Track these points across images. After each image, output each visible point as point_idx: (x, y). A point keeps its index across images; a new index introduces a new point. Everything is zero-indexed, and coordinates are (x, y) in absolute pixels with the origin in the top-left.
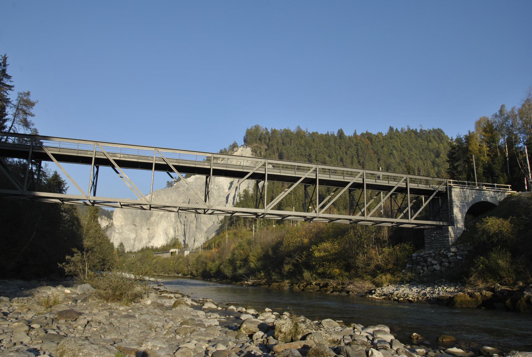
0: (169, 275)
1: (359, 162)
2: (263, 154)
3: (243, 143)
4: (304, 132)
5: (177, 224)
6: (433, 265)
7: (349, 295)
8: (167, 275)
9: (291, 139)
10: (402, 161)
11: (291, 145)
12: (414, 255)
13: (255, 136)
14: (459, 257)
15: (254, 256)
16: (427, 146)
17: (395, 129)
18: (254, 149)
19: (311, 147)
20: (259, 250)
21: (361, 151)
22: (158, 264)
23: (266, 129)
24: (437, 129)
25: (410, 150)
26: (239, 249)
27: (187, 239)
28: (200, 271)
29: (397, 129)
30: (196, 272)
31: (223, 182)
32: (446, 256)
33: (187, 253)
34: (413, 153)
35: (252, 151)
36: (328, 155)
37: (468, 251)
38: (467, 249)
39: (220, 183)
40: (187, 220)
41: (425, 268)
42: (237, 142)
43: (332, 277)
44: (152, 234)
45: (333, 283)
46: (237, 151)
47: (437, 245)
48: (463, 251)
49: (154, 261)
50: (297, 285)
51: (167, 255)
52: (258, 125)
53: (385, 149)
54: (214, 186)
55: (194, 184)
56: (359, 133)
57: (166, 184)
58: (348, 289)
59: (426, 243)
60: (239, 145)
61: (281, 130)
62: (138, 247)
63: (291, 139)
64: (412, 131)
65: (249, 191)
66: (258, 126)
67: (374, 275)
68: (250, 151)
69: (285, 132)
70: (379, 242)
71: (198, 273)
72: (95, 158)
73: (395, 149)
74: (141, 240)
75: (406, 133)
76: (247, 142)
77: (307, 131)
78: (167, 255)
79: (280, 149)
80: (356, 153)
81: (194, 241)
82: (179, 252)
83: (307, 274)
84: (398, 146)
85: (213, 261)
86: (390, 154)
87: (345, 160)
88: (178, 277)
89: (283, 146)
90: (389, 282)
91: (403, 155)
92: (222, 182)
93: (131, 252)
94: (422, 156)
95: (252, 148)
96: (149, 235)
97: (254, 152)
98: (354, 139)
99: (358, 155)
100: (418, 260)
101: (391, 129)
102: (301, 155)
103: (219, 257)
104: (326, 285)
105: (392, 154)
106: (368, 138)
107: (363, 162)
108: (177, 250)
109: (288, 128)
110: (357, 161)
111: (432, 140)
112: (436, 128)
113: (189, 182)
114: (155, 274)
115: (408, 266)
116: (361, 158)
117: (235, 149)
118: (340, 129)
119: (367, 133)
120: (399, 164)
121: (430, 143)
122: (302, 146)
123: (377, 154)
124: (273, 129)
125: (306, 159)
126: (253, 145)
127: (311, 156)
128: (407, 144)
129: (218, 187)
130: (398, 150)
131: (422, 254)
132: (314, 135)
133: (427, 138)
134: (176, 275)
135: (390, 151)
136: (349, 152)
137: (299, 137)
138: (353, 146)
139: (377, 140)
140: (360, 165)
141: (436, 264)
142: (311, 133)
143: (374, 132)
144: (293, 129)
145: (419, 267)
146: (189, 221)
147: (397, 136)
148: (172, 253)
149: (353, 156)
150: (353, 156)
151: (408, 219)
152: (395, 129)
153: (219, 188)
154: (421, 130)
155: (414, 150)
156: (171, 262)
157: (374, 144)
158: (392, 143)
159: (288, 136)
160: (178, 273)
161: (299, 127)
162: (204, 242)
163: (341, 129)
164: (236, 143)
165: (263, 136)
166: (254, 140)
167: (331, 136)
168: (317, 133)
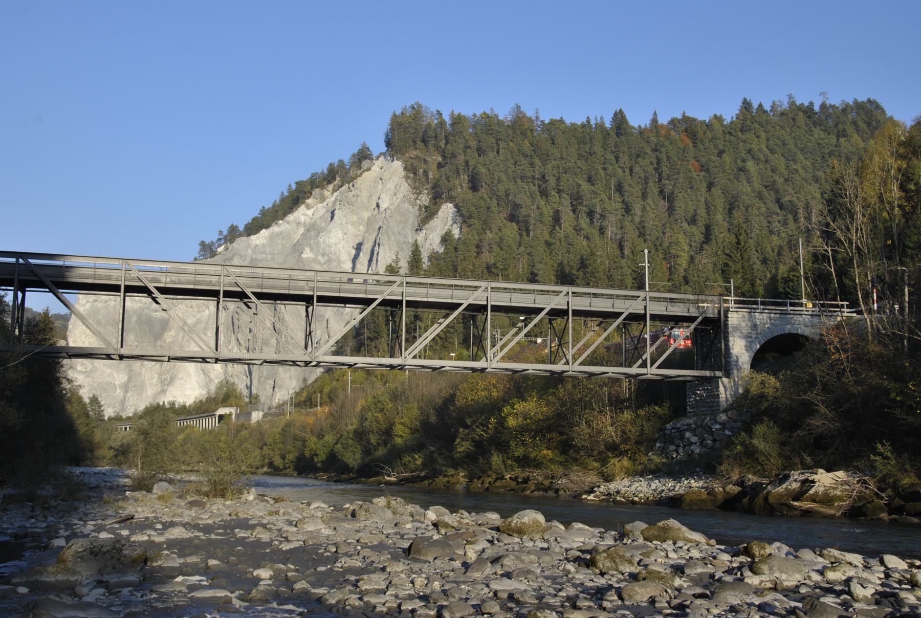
1: (661, 192)
2: (431, 176)
3: (384, 149)
4: (530, 119)
5: (230, 347)
6: (691, 443)
7: (558, 497)
9: (500, 139)
10: (766, 187)
11: (498, 153)
12: (668, 426)
13: (412, 131)
14: (727, 432)
16: (836, 146)
17: (755, 105)
18: (412, 165)
19: (545, 160)
20: (415, 412)
21: (669, 165)
22: (189, 445)
23: (439, 113)
24: (865, 100)
25: (790, 158)
26: (373, 411)
27: (255, 382)
28: (291, 457)
29: (760, 106)
30: (282, 461)
31: (338, 246)
32: (710, 432)
33: (256, 416)
34: (798, 166)
35: (405, 169)
37: (742, 421)
38: (743, 419)
40: (254, 336)
41: (681, 450)
43: (538, 465)
44: (168, 372)
46: (369, 169)
48: (735, 421)
49: (181, 437)
50: (480, 481)
51: (210, 423)
52: (420, 103)
53: (727, 158)
55: (267, 250)
56: (663, 120)
57: (198, 248)
58: (556, 487)
59: (689, 405)
60: (375, 153)
61: (475, 115)
62: (137, 404)
64: (800, 108)
66: (420, 106)
67: (604, 461)
68: (401, 169)
69: (483, 122)
70: (617, 404)
71: (286, 461)
73: (753, 158)
74: (141, 388)
75: (783, 114)
76: (393, 146)
78: (210, 423)
79: (472, 163)
80: (655, 169)
81: (274, 387)
82: (238, 416)
83: (496, 459)
84: (760, 150)
85: (320, 436)
86: (741, 169)
87: (626, 188)
89: (480, 156)
90: (626, 473)
91: (770, 174)
92: (336, 244)
93: (118, 419)
94: (820, 174)
95: (405, 162)
96: (161, 374)
97: (409, 170)
98: (651, 134)
99: (660, 175)
100: (673, 435)
101: (746, 105)
102: (521, 178)
103: (333, 427)
104: (526, 481)
105: (743, 171)
106: (686, 131)
107: (673, 193)
110: (656, 191)
111: (850, 129)
112: (862, 98)
115: (658, 445)
116: (667, 182)
117: (365, 164)
119: (685, 119)
120: (760, 196)
121: (842, 140)
122: (525, 156)
123: (708, 171)
124: (456, 113)
125: (534, 188)
127: (547, 181)
128: (784, 144)
129: (326, 258)
130: (759, 159)
131: (679, 425)
132: (555, 125)
133: (836, 125)
135: (740, 164)
136: (637, 169)
137: (518, 132)
138: (648, 151)
139: (709, 134)
140: (664, 199)
141: (695, 443)
142: (547, 122)
143: (702, 114)
144: (504, 113)
145: (673, 447)
146: (260, 340)
147: (760, 124)
148: (221, 417)
149: (646, 178)
150: (646, 178)
151: (646, 367)
152: (755, 105)
154: (823, 106)
155: (801, 157)
157: (700, 146)
158: (745, 142)
159: (491, 132)
161: (518, 107)
162: (297, 390)
163: (621, 110)
164: (368, 149)
165: (431, 133)
166: (411, 143)
167: (596, 128)
168: (561, 121)
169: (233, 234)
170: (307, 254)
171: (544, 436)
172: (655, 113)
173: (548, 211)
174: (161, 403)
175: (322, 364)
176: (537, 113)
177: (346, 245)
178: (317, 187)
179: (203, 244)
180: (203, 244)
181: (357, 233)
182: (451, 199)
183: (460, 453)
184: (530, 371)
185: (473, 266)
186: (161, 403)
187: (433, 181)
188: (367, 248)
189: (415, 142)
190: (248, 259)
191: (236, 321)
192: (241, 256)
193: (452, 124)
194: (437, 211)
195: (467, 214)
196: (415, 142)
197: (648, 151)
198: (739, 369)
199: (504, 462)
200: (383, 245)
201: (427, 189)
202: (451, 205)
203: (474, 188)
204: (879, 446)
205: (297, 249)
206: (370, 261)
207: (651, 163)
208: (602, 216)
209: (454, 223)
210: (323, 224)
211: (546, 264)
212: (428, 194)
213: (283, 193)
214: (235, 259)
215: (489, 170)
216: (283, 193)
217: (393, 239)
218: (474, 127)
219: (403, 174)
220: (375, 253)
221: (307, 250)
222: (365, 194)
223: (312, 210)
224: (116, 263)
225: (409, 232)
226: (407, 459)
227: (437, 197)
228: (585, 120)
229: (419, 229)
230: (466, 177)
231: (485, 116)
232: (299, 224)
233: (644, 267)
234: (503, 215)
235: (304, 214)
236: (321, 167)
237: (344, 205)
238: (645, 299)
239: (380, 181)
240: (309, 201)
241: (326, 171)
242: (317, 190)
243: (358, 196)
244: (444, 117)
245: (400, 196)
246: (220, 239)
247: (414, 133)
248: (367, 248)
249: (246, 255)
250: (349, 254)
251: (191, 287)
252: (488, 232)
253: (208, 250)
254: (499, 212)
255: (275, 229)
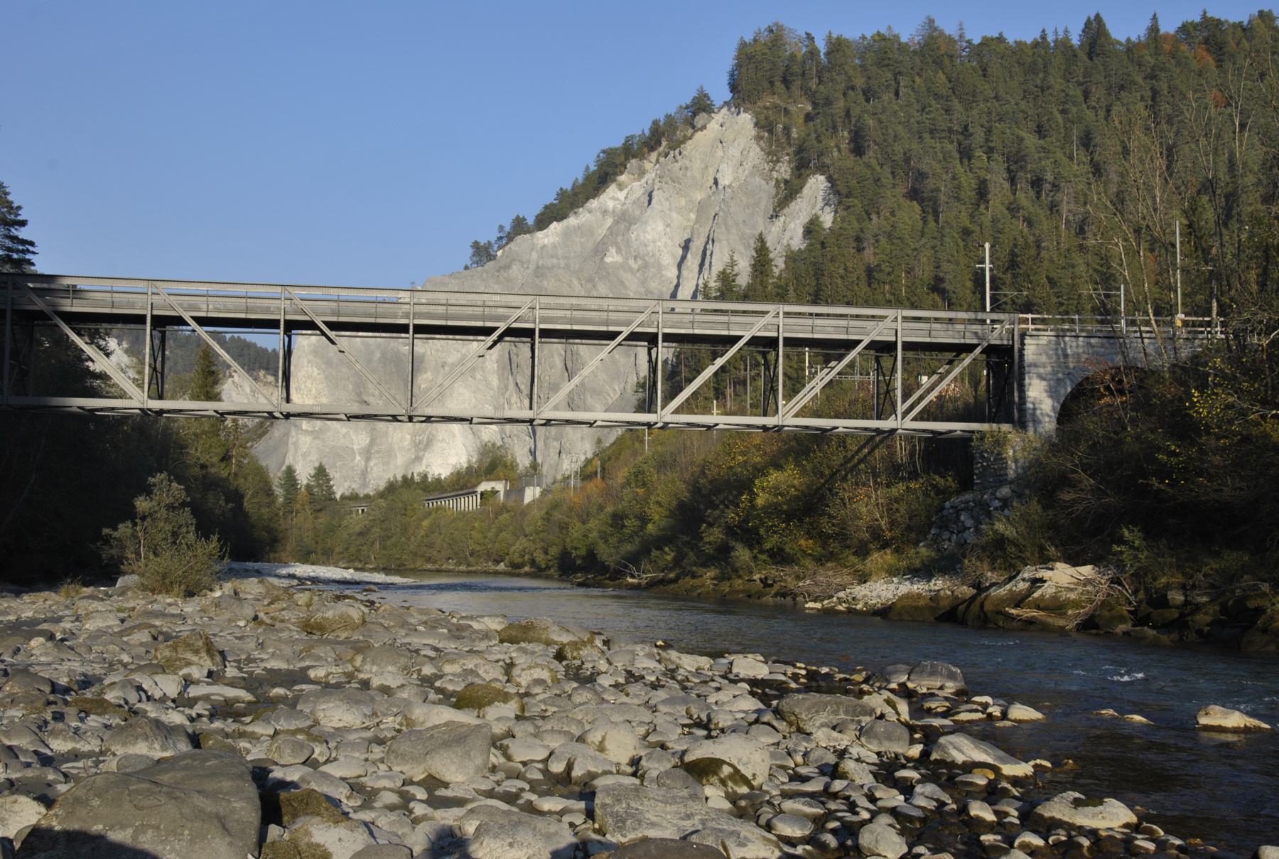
0: (470, 568)
2: (794, 135)
3: (728, 96)
4: (950, 40)
5: (507, 395)
8: (463, 568)
9: (900, 73)
11: (897, 94)
13: (767, 66)
15: (661, 506)
18: (766, 119)
19: (970, 99)
27: (540, 445)
28: (554, 551)
31: (659, 244)
33: (531, 494)
35: (756, 125)
36: (1032, 125)
39: (646, 246)
42: (707, 90)
45: (786, 575)
46: (704, 128)
49: (426, 523)
51: (469, 504)
52: (780, 23)
54: (627, 259)
55: (560, 252)
56: (1169, 26)
57: (470, 251)
60: (718, 102)
61: (864, 38)
62: (379, 476)
63: (900, 73)
65: (736, 275)
69: (877, 45)
70: (895, 471)
72: (153, 316)
74: (389, 454)
77: (961, 36)
78: (469, 504)
79: (855, 111)
81: (560, 452)
82: (507, 493)
83: (742, 554)
87: (1098, 140)
88: (497, 573)
89: (868, 100)
92: (654, 242)
93: (354, 497)
95: (756, 114)
97: (762, 127)
98: (1146, 52)
102: (931, 132)
108: (499, 486)
109: (890, 28)
113: (544, 246)
114: (429, 566)
115: (933, 531)
117: (700, 120)
118: (1092, 18)
122: (937, 97)
124: (835, 36)
125: (950, 147)
126: (759, 104)
127: (971, 135)
129: (640, 262)
134: (491, 566)
137: (930, 60)
138: (1139, 79)
142: (976, 41)
144: (908, 32)
146: (546, 385)
148: (482, 494)
153: (646, 266)
156: (476, 525)
159: (886, 62)
160: (497, 562)
161: (931, 21)
162: (590, 455)
163: (1098, 17)
164: (706, 95)
165: (796, 69)
166: (766, 84)
167: (1056, 47)
168: (1001, 39)
169: (520, 227)
170: (612, 257)
171: (801, 521)
172: (1155, 18)
173: (968, 183)
174: (409, 476)
175: (423, 419)
176: (961, 29)
177: (669, 243)
178: (634, 157)
179: (476, 245)
180: (476, 245)
181: (685, 223)
182: (822, 169)
183: (710, 543)
184: (840, 429)
185: (846, 269)
186: (409, 476)
187: (797, 142)
188: (697, 246)
189: (772, 83)
190: (532, 267)
191: (514, 357)
192: (522, 263)
193: (828, 54)
194: (801, 188)
195: (844, 191)
196: (772, 83)
197: (1139, 79)
198: (1036, 421)
199: (755, 558)
200: (720, 241)
201: (788, 154)
202: (822, 178)
203: (858, 150)
204: (1126, 533)
205: (600, 251)
206: (702, 265)
207: (1142, 98)
208: (1054, 185)
209: (826, 204)
210: (637, 213)
211: (958, 264)
212: (789, 162)
213: (587, 168)
214: (514, 267)
215: (881, 122)
216: (587, 168)
217: (734, 231)
218: (862, 58)
219: (754, 132)
220: (708, 253)
221: (613, 250)
222: (697, 165)
223: (625, 191)
224: (142, 286)
225: (760, 221)
226: (655, 553)
227: (803, 168)
228: (1037, 35)
229: (774, 216)
230: (846, 134)
231: (880, 38)
232: (605, 212)
233: (983, 270)
234: (901, 190)
235: (614, 199)
236: (641, 127)
237: (667, 183)
238: (896, 320)
239: (720, 145)
240: (622, 178)
241: (647, 133)
242: (634, 161)
243: (686, 168)
244: (817, 43)
245: (748, 166)
246: (500, 238)
247: (771, 69)
248: (697, 246)
249: (529, 261)
250: (674, 256)
251: (242, 316)
252: (874, 217)
253: (482, 253)
254: (894, 186)
255: (572, 221)
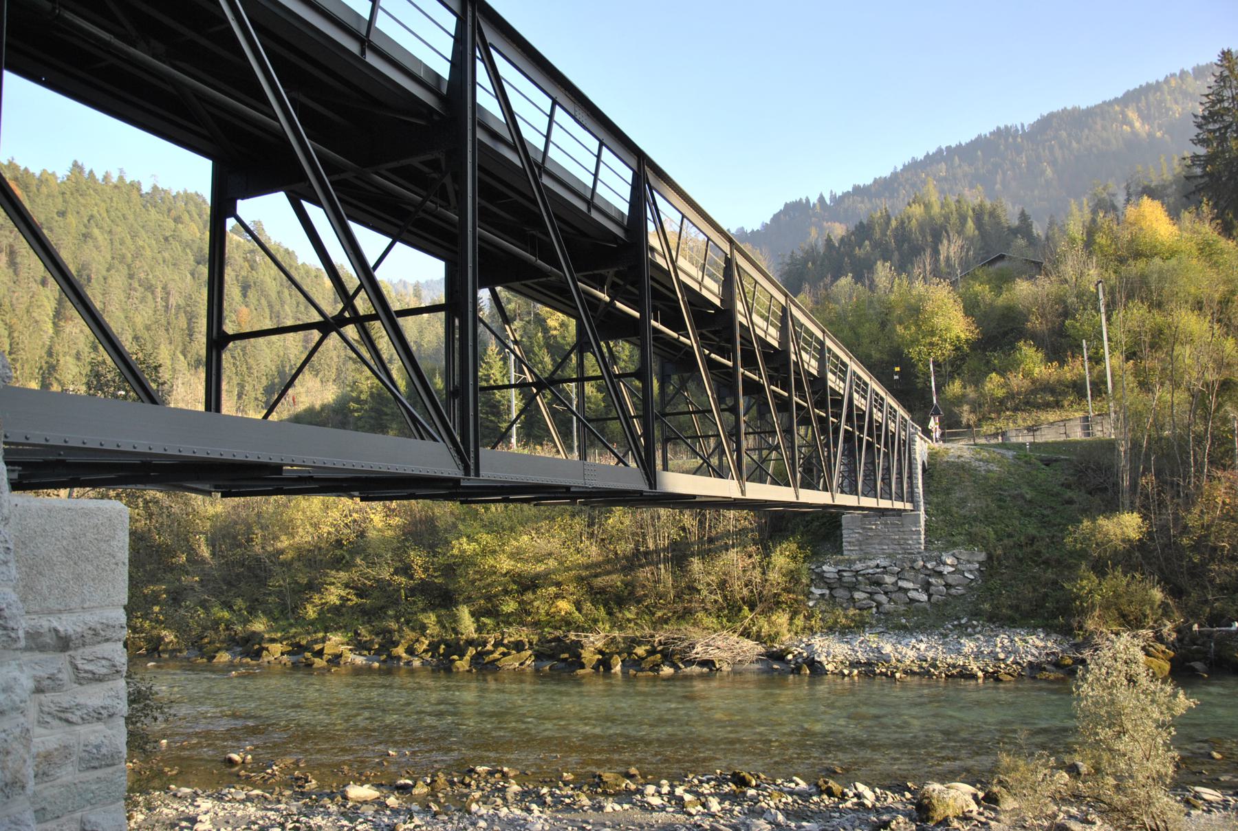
17: (87, 170)
24: (193, 192)
29: (91, 172)
37: (979, 563)
47: (885, 547)
53: (72, 219)
75: (116, 187)
101: (76, 166)
111: (186, 217)
112: (191, 190)
121: (180, 226)
135: (84, 230)
139: (44, 190)
147: (95, 190)
154: (155, 188)
158: (84, 206)
